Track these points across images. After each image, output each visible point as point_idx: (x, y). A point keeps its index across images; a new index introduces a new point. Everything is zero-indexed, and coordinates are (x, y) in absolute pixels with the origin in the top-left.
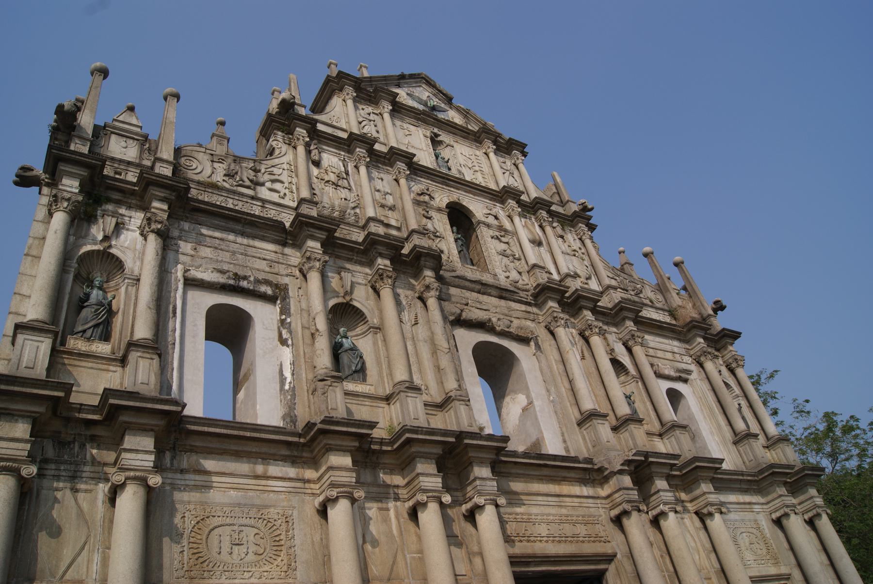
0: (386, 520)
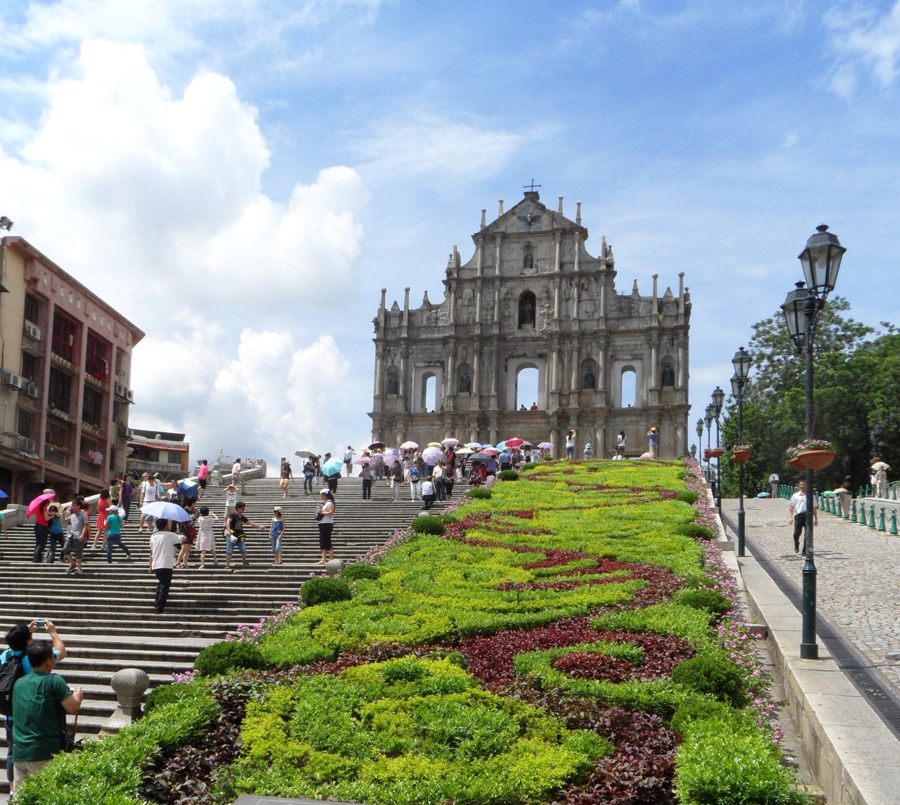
0: (465, 434)
